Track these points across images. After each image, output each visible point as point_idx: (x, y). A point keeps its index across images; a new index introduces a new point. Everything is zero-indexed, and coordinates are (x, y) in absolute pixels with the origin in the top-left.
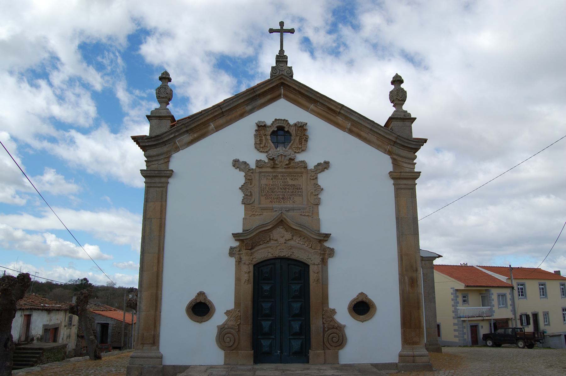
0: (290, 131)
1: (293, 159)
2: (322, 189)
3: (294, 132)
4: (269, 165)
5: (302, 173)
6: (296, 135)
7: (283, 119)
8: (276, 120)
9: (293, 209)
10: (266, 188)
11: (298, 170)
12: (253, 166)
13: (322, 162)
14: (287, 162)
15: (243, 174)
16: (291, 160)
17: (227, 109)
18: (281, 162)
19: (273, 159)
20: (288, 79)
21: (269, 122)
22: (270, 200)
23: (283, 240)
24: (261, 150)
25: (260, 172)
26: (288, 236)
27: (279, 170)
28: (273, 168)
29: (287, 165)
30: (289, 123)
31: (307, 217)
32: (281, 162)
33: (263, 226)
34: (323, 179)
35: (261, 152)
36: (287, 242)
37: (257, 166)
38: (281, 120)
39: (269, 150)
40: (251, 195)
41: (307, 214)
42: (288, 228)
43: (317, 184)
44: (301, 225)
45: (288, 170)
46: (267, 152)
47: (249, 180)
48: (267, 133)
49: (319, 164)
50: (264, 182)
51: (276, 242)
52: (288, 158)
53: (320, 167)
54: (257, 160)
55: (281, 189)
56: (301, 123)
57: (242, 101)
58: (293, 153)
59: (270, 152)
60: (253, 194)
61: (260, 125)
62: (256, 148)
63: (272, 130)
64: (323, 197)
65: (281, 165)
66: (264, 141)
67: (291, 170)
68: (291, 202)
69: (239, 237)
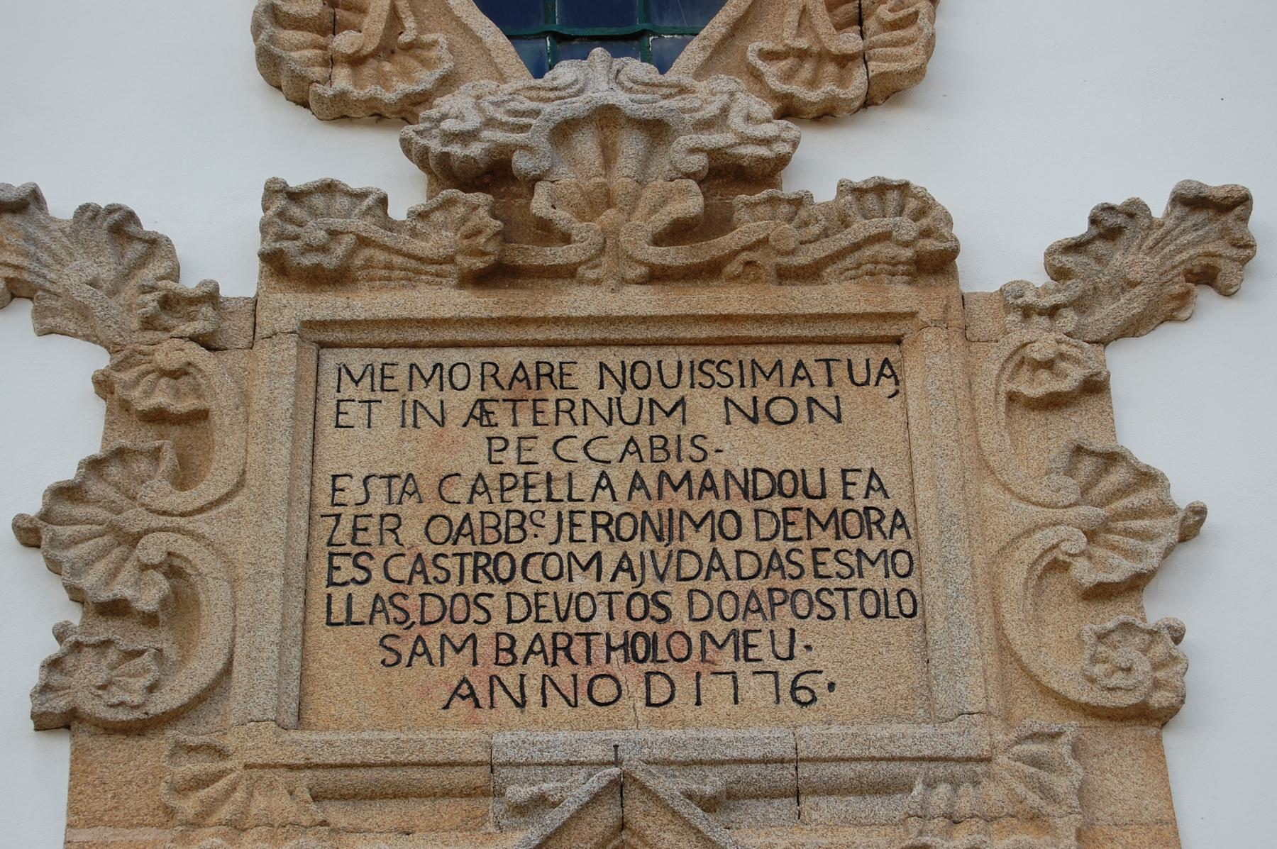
2: (1192, 524)
5: (887, 335)
10: (392, 524)
11: (839, 295)
12: (218, 247)
14: (691, 203)
15: (83, 360)
16: (730, 175)
19: (496, 176)
22: (457, 666)
25: (320, 337)
27: (579, 301)
29: (678, 232)
35: (340, 113)
39: (447, 83)
40: (180, 606)
43: (1112, 458)
46: (408, 109)
47: (158, 427)
49: (1111, 225)
50: (368, 444)
52: (686, 152)
53: (1125, 259)
54: (275, 190)
55: (608, 526)
60: (214, 596)
62: (269, 63)
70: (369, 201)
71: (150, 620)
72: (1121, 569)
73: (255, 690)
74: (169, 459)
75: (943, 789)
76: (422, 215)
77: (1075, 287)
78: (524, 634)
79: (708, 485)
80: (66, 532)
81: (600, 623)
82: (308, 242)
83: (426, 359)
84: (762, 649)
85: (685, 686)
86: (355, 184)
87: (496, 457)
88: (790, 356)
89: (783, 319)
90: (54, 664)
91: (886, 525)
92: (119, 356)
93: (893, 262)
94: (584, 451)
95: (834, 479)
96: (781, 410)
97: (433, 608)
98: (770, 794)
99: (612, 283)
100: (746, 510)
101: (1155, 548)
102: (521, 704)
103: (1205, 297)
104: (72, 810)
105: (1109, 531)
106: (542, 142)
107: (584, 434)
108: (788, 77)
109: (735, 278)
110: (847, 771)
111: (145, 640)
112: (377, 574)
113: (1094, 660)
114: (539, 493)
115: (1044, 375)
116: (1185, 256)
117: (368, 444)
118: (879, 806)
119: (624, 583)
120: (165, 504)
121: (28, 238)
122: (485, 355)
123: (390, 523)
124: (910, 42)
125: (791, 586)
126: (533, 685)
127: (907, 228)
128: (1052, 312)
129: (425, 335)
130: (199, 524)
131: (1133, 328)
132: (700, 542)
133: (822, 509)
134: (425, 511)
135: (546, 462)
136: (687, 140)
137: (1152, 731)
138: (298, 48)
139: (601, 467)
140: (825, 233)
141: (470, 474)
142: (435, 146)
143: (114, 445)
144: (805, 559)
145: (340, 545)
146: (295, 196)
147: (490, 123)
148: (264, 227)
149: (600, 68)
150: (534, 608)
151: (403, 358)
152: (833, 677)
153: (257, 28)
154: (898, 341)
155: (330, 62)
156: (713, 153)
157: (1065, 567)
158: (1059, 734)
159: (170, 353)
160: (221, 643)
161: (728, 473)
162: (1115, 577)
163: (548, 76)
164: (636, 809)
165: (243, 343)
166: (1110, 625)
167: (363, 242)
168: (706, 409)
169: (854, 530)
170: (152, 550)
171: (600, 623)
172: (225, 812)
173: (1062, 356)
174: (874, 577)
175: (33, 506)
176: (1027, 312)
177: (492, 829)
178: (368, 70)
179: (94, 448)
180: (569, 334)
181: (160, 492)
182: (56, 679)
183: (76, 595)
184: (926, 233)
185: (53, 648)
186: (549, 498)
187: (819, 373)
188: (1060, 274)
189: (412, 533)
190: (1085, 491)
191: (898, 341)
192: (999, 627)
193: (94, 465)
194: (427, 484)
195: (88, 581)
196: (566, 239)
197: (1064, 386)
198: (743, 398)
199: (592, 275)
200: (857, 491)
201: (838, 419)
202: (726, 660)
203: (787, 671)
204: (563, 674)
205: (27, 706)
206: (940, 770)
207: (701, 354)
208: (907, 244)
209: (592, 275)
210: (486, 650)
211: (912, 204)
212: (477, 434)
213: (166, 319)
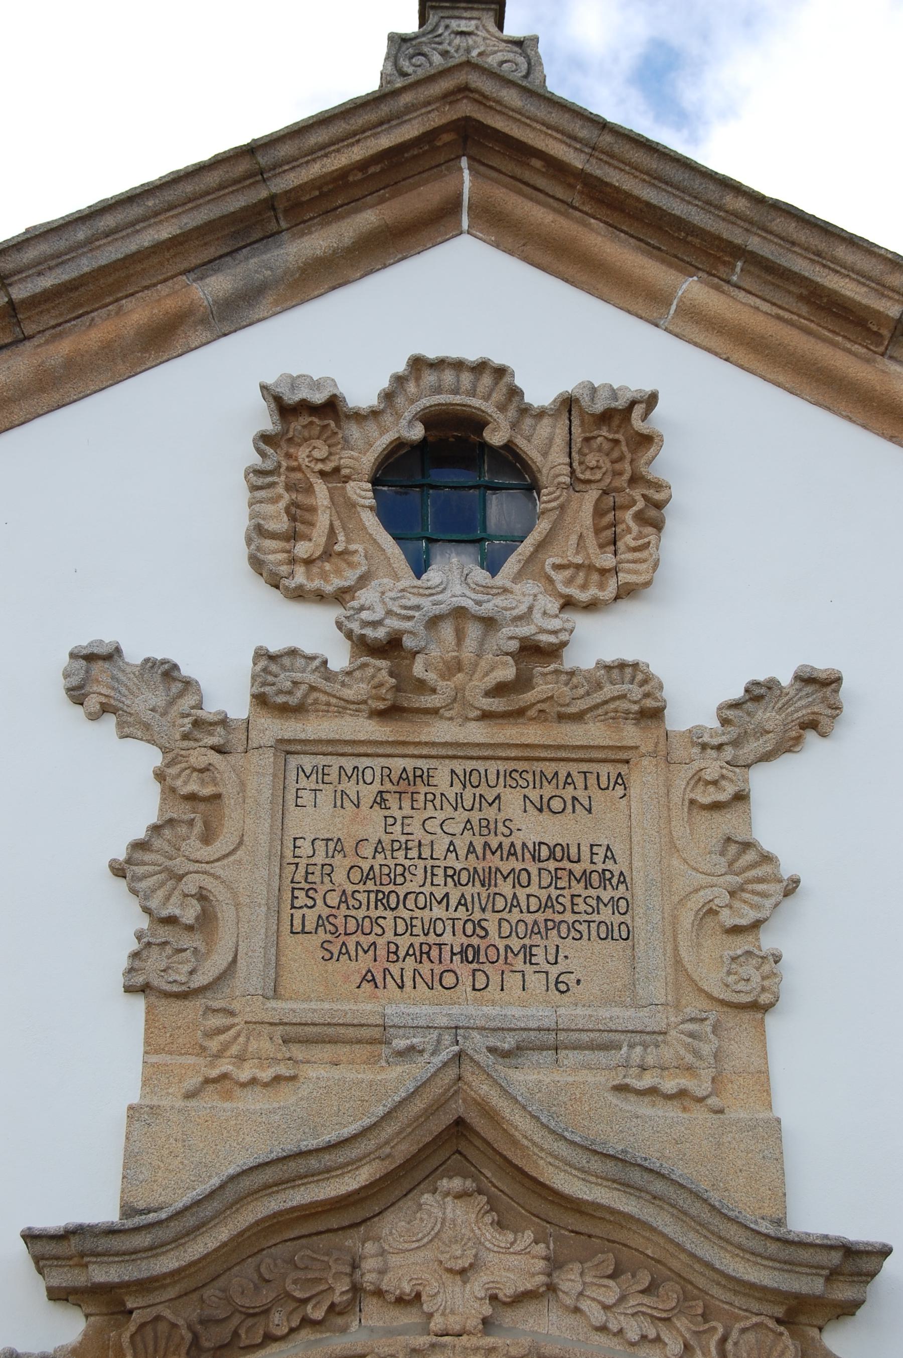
0: (531, 450)
1: (553, 652)
2: (792, 887)
3: (558, 456)
4: (357, 690)
5: (621, 756)
6: (576, 483)
7: (472, 356)
8: (418, 364)
9: (552, 1042)
10: (328, 870)
11: (593, 733)
12: (227, 691)
13: (786, 679)
14: (507, 672)
15: (146, 757)
16: (534, 652)
17: (47, 282)
18: (454, 667)
19: (392, 647)
20: (511, 97)
21: (362, 391)
23: (461, 1303)
24: (300, 577)
25: (286, 748)
26: (513, 1261)
27: (441, 731)
28: (391, 712)
29: (500, 690)
30: (515, 393)
31: (671, 1112)
32: (454, 667)
33: (291, 1166)
34: (788, 806)
35: (299, 595)
36: (508, 1318)
37: (260, 700)
38: (458, 365)
39: (364, 580)
40: (207, 921)
41: (670, 1085)
42: (519, 1193)
43: (747, 845)
44: (624, 1168)
45: (511, 733)
46: (341, 597)
48: (345, 459)
49: (758, 693)
50: (315, 818)
51: (407, 1318)
52: (507, 637)
54: (261, 654)
55: (453, 876)
56: (614, 394)
57: (165, 232)
58: (553, 606)
59: (366, 596)
60: (226, 913)
61: (292, 398)
62: (257, 563)
63: (383, 442)
64: (799, 942)
65: (458, 696)
66: (323, 520)
68: (535, 982)
69: (82, 1259)
71: (190, 928)
72: (748, 916)
74: (199, 827)
75: (639, 1049)
76: (349, 673)
77: (733, 732)
78: (404, 942)
79: (512, 853)
80: (140, 870)
81: (447, 938)
82: (281, 685)
83: (349, 764)
84: (540, 958)
85: (495, 979)
86: (308, 650)
87: (389, 829)
88: (563, 769)
89: (559, 747)
90: (135, 955)
91: (615, 881)
92: (170, 756)
93: (627, 712)
94: (440, 828)
95: (585, 849)
96: (556, 804)
97: (352, 925)
98: (542, 1048)
99: (460, 720)
100: (533, 869)
101: (768, 903)
102: (401, 987)
103: (811, 736)
104: (147, 1043)
105: (743, 890)
107: (441, 816)
108: (569, 582)
109: (532, 719)
110: (585, 1037)
111: (187, 941)
112: (320, 902)
113: (729, 973)
114: (413, 853)
115: (711, 789)
116: (800, 714)
117: (315, 818)
118: (601, 1057)
119: (462, 913)
120: (198, 855)
121: (113, 678)
122: (383, 761)
123: (327, 869)
124: (645, 561)
125: (558, 918)
126: (408, 975)
127: (636, 692)
128: (719, 747)
129: (348, 749)
130: (217, 868)
131: (767, 757)
132: (506, 888)
133: (577, 869)
134: (348, 863)
135: (419, 834)
136: (507, 631)
137: (760, 1016)
138: (274, 552)
139: (450, 838)
140: (588, 694)
141: (374, 840)
142: (355, 626)
143: (167, 816)
144: (566, 901)
145: (298, 883)
146: (273, 658)
147: (389, 613)
148: (254, 677)
149: (456, 577)
150: (410, 926)
152: (579, 976)
153: (249, 541)
154: (627, 762)
155: (293, 561)
156: (522, 640)
157: (716, 913)
158: (706, 1019)
159: (200, 757)
160: (231, 944)
161: (524, 844)
162: (744, 922)
163: (424, 577)
164: (468, 1071)
165: (241, 749)
166: (739, 952)
167: (313, 688)
168: (512, 800)
169: (596, 884)
170: (190, 885)
171: (447, 938)
172: (234, 1050)
173: (723, 777)
174: (606, 914)
175: (121, 855)
176: (704, 747)
177: (384, 1064)
178: (315, 570)
179: (153, 818)
180: (434, 752)
181: (194, 847)
182: (137, 964)
183: (147, 910)
184: (647, 695)
185: (135, 946)
186: (420, 857)
187: (579, 781)
188: (725, 722)
189: (340, 876)
190: (730, 864)
191: (627, 762)
192: (676, 949)
193: (155, 829)
194: (349, 845)
195: (153, 904)
196: (434, 691)
197: (723, 797)
198: (534, 795)
199: (448, 714)
200: (598, 859)
201: (590, 811)
202: (519, 963)
203: (554, 971)
204: (425, 968)
205: (120, 981)
206: (637, 1038)
207: (511, 765)
208: (635, 702)
209: (448, 714)
210: (382, 952)
211: (640, 677)
212: (378, 814)
213: (197, 734)
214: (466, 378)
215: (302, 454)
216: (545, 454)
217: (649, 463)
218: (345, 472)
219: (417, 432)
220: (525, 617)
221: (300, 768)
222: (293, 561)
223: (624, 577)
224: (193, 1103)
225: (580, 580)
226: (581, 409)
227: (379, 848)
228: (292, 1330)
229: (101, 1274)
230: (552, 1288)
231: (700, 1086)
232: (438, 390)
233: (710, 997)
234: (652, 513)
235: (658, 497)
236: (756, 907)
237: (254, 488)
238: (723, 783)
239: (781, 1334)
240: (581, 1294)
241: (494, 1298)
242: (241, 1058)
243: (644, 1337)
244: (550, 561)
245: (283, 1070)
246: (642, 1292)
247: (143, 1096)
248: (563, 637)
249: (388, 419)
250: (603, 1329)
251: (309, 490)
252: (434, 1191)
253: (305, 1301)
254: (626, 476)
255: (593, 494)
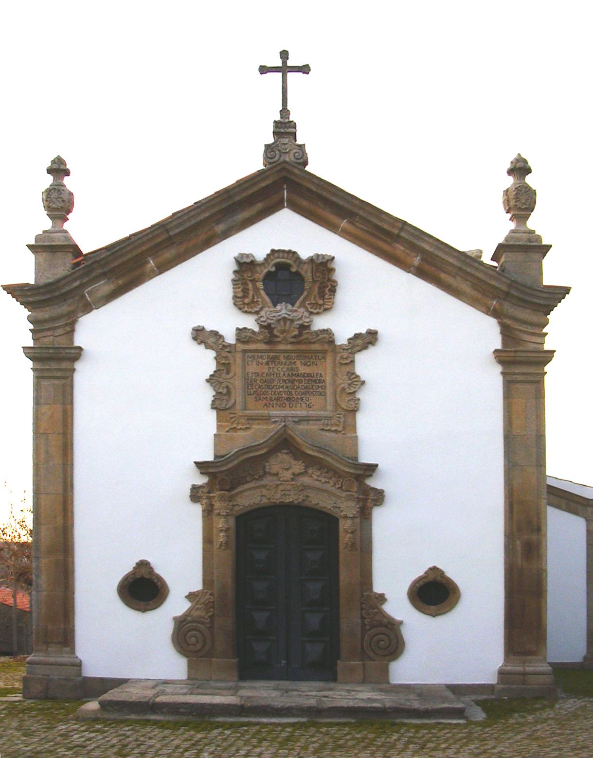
1: (308, 327)
2: (363, 383)
3: (309, 275)
5: (324, 352)
6: (314, 281)
7: (287, 249)
8: (273, 251)
10: (256, 381)
12: (230, 338)
14: (296, 333)
15: (212, 354)
23: (288, 475)
24: (246, 309)
25: (245, 351)
26: (298, 467)
27: (282, 347)
28: (269, 342)
29: (295, 337)
31: (334, 434)
32: (283, 332)
35: (246, 312)
37: (238, 340)
38: (283, 251)
39: (261, 309)
40: (229, 393)
41: (333, 429)
43: (353, 373)
47: (223, 366)
48: (257, 276)
49: (357, 336)
50: (253, 368)
51: (275, 478)
53: (359, 342)
54: (238, 329)
55: (284, 381)
56: (323, 256)
59: (262, 313)
60: (233, 391)
63: (265, 271)
64: (364, 396)
66: (251, 293)
67: (303, 347)
68: (304, 405)
70: (250, 331)
71: (225, 395)
72: (352, 390)
73: (239, 406)
74: (225, 372)
79: (298, 376)
80: (212, 381)
81: (283, 395)
83: (260, 354)
85: (294, 405)
86: (249, 328)
88: (310, 355)
90: (213, 401)
94: (281, 370)
95: (315, 375)
96: (308, 363)
97: (262, 393)
98: (305, 420)
100: (303, 379)
101: (358, 387)
102: (273, 407)
104: (217, 419)
106: (275, 322)
107: (281, 367)
108: (311, 308)
113: (348, 403)
114: (275, 376)
115: (345, 360)
118: (318, 423)
119: (286, 390)
121: (203, 335)
124: (330, 302)
126: (275, 404)
128: (347, 349)
130: (230, 381)
131: (359, 351)
132: (297, 384)
138: (240, 302)
143: (219, 368)
144: (311, 387)
145: (248, 383)
147: (268, 318)
148: (236, 335)
149: (284, 307)
150: (275, 393)
151: (256, 354)
152: (313, 404)
153: (233, 299)
157: (345, 389)
159: (224, 354)
160: (234, 398)
161: (301, 373)
163: (277, 307)
165: (234, 351)
167: (250, 337)
168: (298, 363)
170: (224, 385)
171: (283, 395)
172: (236, 422)
173: (348, 357)
174: (320, 390)
175: (208, 377)
179: (215, 369)
183: (215, 390)
184: (330, 337)
185: (213, 399)
186: (277, 377)
187: (314, 358)
188: (349, 343)
192: (336, 398)
193: (215, 372)
194: (260, 374)
195: (216, 389)
196: (278, 337)
198: (303, 362)
200: (318, 377)
201: (316, 365)
203: (308, 403)
204: (279, 403)
205: (210, 407)
206: (327, 418)
211: (328, 333)
212: (266, 367)
214: (286, 255)
215: (245, 275)
216: (306, 272)
217: (332, 276)
218: (256, 280)
219: (273, 269)
220: (301, 319)
221: (248, 356)
222: (244, 304)
223: (326, 306)
224: (228, 433)
225: (314, 307)
226: (314, 262)
227: (267, 375)
228: (252, 480)
229: (211, 470)
230: (306, 472)
231: (340, 429)
232: (278, 258)
233: (343, 409)
234: (333, 289)
235: (335, 285)
236: (355, 388)
237: (234, 285)
238: (348, 358)
239: (354, 481)
240: (312, 473)
241: (294, 474)
242: (238, 423)
243: (326, 482)
244: (307, 303)
245: (248, 426)
246: (325, 473)
247: (217, 432)
248: (310, 324)
249: (266, 265)
250: (317, 480)
251: (247, 284)
252: (281, 452)
253: (253, 475)
254: (327, 279)
255: (318, 284)
